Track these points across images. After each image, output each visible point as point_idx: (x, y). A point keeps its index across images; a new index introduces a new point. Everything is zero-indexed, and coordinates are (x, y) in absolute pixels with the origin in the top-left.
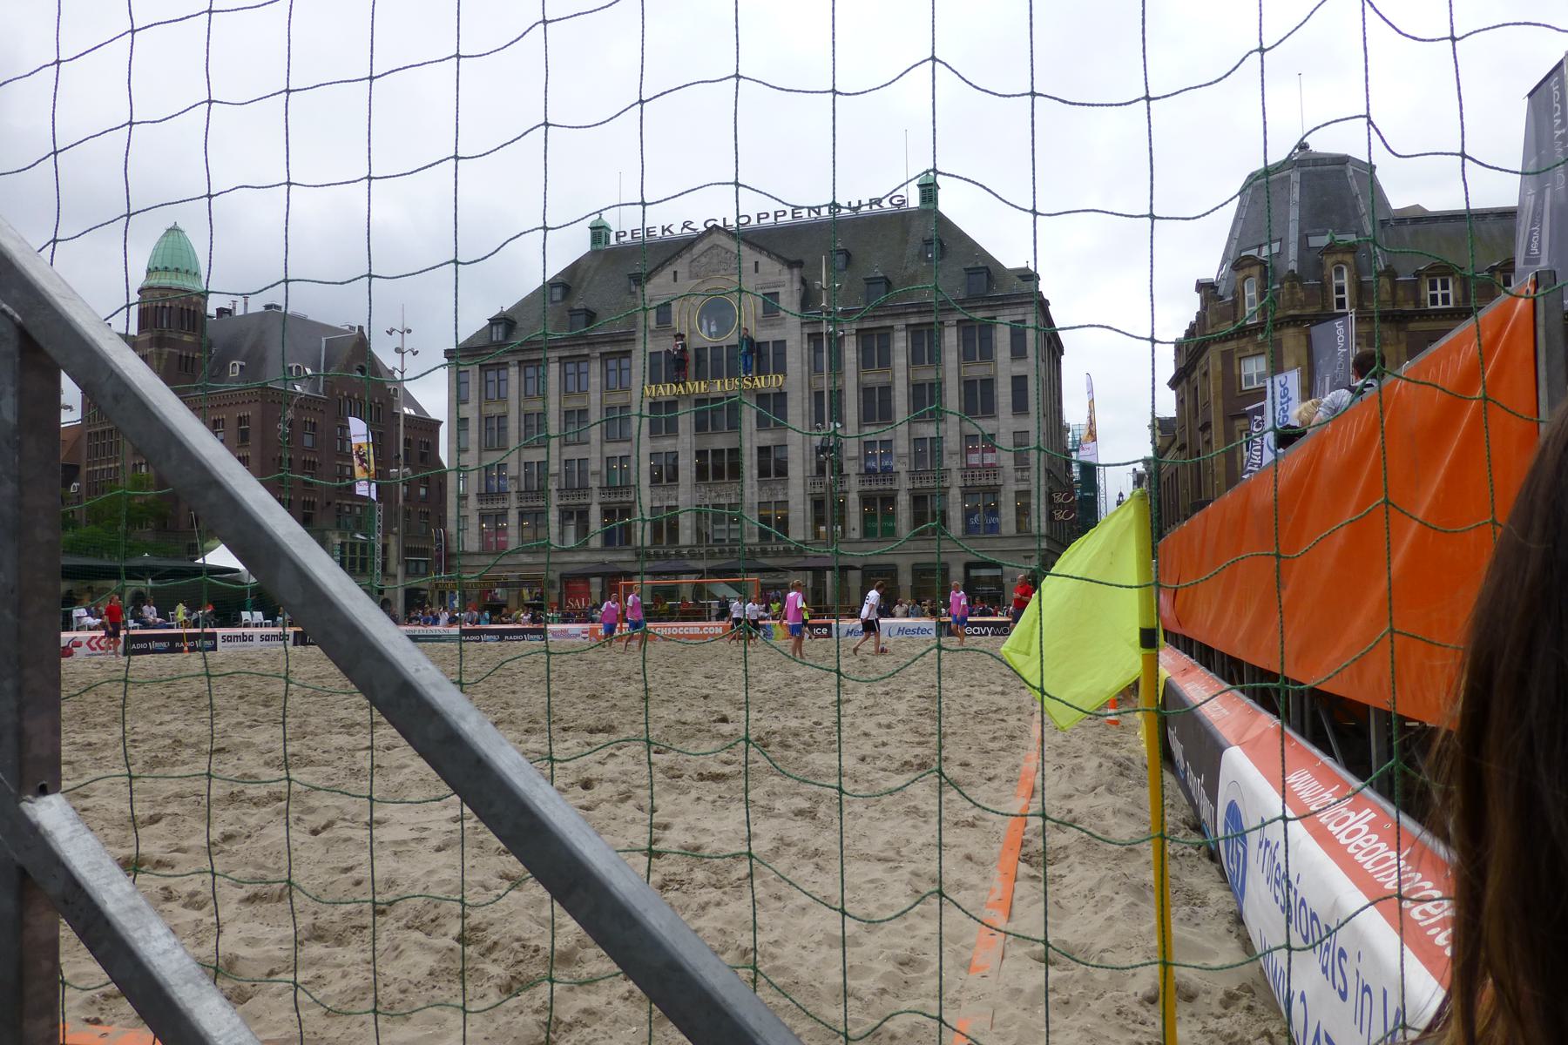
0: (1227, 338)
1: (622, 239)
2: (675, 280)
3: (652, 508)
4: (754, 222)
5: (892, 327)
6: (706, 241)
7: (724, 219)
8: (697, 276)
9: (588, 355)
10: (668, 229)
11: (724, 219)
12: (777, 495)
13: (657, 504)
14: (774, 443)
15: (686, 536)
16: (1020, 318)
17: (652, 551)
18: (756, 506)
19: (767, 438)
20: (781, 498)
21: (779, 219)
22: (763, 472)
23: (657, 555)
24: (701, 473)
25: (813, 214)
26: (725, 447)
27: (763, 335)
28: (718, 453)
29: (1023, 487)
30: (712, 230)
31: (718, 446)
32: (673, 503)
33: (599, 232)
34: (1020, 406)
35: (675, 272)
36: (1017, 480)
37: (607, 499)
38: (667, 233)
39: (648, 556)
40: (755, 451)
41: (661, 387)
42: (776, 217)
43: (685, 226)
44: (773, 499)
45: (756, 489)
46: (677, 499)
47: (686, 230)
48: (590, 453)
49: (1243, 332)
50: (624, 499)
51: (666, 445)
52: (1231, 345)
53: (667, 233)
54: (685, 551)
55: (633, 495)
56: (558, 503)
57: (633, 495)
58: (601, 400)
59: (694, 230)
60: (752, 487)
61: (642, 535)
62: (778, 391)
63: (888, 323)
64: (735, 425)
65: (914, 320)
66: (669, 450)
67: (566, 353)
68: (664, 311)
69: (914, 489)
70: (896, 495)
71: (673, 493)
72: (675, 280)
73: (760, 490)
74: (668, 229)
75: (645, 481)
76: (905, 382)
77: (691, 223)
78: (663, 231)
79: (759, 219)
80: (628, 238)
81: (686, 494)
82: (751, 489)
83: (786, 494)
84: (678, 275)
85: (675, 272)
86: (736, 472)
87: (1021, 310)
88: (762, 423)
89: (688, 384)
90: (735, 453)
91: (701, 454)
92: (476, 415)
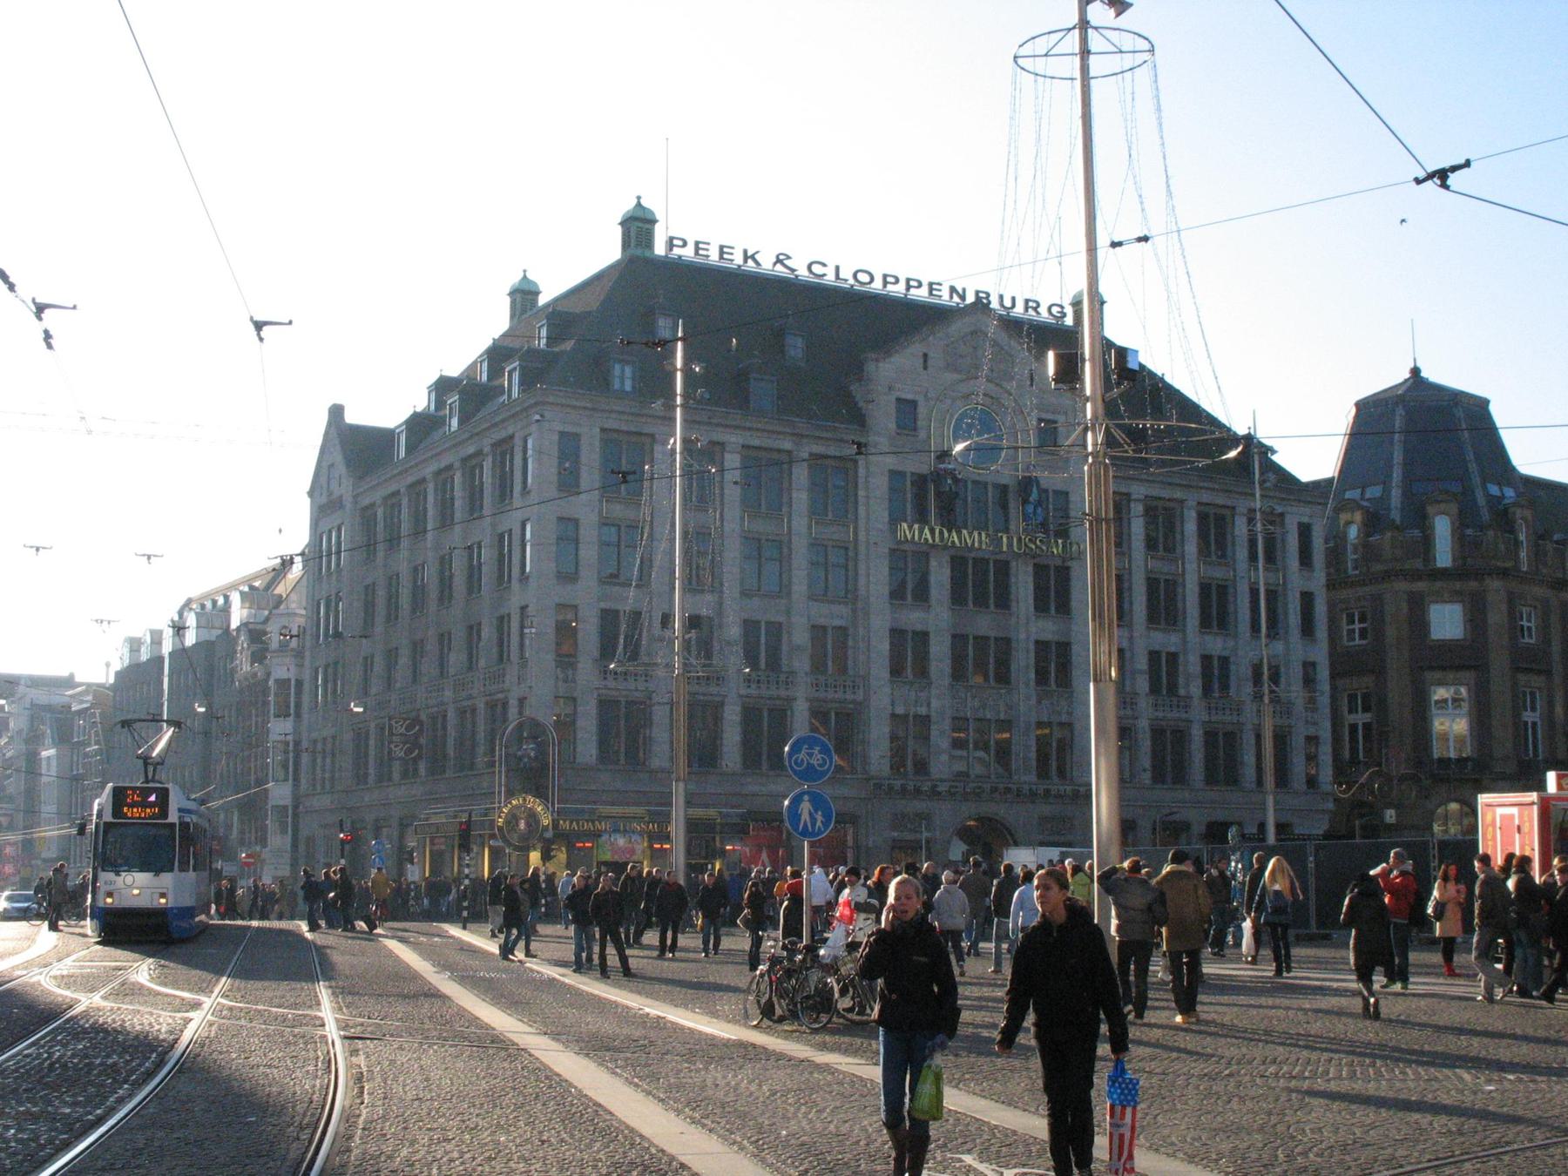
0: (1416, 576)
1: (677, 251)
2: (925, 368)
3: (893, 715)
4: (877, 285)
5: (1182, 502)
6: (967, 320)
7: (837, 268)
8: (956, 370)
9: (789, 452)
10: (753, 257)
11: (837, 268)
12: (1060, 714)
13: (900, 710)
14: (1056, 638)
15: (942, 765)
16: (1305, 520)
17: (898, 783)
18: (1033, 726)
19: (1047, 629)
20: (1064, 718)
21: (913, 291)
22: (1042, 676)
23: (904, 791)
24: (958, 673)
25: (956, 299)
26: (992, 634)
27: (1047, 479)
28: (981, 641)
29: (1312, 731)
30: (981, 304)
31: (982, 633)
32: (923, 711)
33: (638, 225)
34: (1307, 629)
35: (925, 355)
36: (1307, 722)
37: (822, 695)
38: (750, 263)
39: (891, 788)
40: (1032, 647)
41: (926, 531)
42: (908, 287)
43: (778, 261)
44: (1055, 719)
45: (1033, 701)
46: (929, 705)
47: (779, 267)
48: (788, 613)
49: (1444, 574)
50: (850, 696)
51: (913, 618)
52: (1420, 586)
53: (750, 263)
54: (942, 788)
55: (861, 692)
56: (743, 692)
57: (861, 692)
58: (810, 527)
59: (793, 270)
60: (1028, 698)
61: (878, 755)
62: (1059, 562)
63: (1178, 494)
64: (1004, 601)
65: (1206, 497)
66: (919, 627)
67: (756, 442)
68: (907, 410)
69: (1210, 722)
70: (1189, 728)
71: (923, 695)
72: (925, 368)
73: (1039, 702)
74: (753, 257)
75: (879, 670)
76: (1196, 578)
77: (789, 257)
78: (746, 258)
79: (885, 283)
80: (688, 253)
81: (939, 700)
82: (1024, 699)
83: (1070, 714)
84: (930, 363)
85: (925, 355)
86: (1003, 677)
87: (1308, 510)
88: (1041, 606)
89: (965, 532)
90: (1005, 644)
91: (959, 639)
92: (594, 518)
